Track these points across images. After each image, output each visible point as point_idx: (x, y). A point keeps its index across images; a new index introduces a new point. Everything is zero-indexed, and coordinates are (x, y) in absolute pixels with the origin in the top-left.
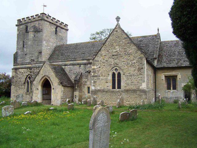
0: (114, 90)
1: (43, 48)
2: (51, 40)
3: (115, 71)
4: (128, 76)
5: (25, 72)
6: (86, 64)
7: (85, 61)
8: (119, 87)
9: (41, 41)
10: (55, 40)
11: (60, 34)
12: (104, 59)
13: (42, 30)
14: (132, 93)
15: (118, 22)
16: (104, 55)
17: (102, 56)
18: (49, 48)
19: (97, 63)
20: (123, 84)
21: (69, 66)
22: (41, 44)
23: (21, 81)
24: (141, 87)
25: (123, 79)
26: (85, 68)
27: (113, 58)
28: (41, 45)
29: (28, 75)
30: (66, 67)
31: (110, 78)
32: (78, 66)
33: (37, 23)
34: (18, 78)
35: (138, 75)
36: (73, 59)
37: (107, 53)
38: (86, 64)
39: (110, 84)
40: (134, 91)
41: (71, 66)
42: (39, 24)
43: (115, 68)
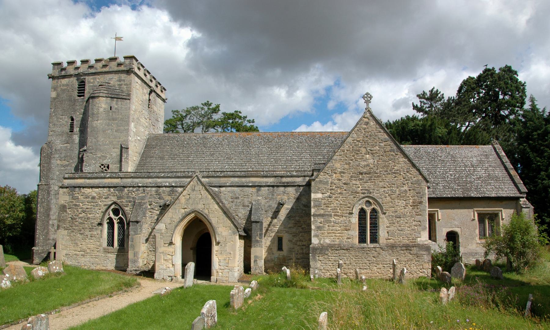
0: (363, 245)
1: (130, 138)
2: (143, 120)
3: (364, 207)
4: (392, 216)
5: (100, 197)
6: (273, 186)
7: (270, 180)
8: (374, 239)
9: (126, 121)
10: (148, 120)
11: (155, 108)
12: (339, 180)
13: (129, 95)
14: (402, 252)
15: (368, 105)
16: (339, 170)
17: (335, 173)
18: (139, 138)
19: (322, 186)
20: (382, 234)
21: (230, 188)
22: (126, 128)
23: (88, 218)
24: (419, 239)
25: (383, 222)
26: (273, 195)
27: (361, 179)
28: (127, 130)
29: (111, 205)
30: (222, 189)
31: (355, 220)
32: (254, 190)
33: (115, 77)
34: (80, 210)
35: (412, 216)
36: (239, 173)
37: (346, 166)
38: (273, 186)
39: (355, 233)
40: (407, 247)
41: (236, 189)
42: (120, 81)
43: (367, 199)
